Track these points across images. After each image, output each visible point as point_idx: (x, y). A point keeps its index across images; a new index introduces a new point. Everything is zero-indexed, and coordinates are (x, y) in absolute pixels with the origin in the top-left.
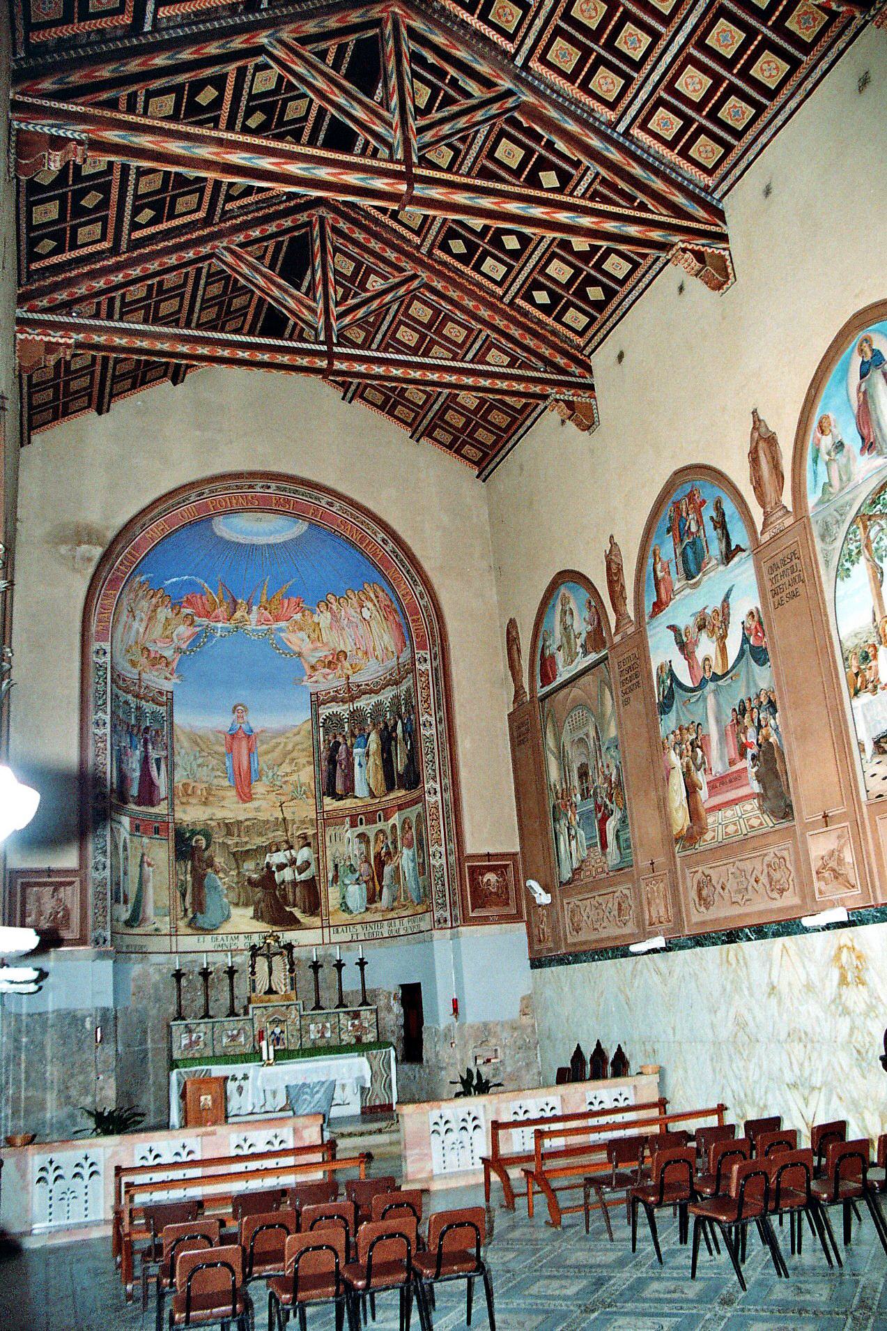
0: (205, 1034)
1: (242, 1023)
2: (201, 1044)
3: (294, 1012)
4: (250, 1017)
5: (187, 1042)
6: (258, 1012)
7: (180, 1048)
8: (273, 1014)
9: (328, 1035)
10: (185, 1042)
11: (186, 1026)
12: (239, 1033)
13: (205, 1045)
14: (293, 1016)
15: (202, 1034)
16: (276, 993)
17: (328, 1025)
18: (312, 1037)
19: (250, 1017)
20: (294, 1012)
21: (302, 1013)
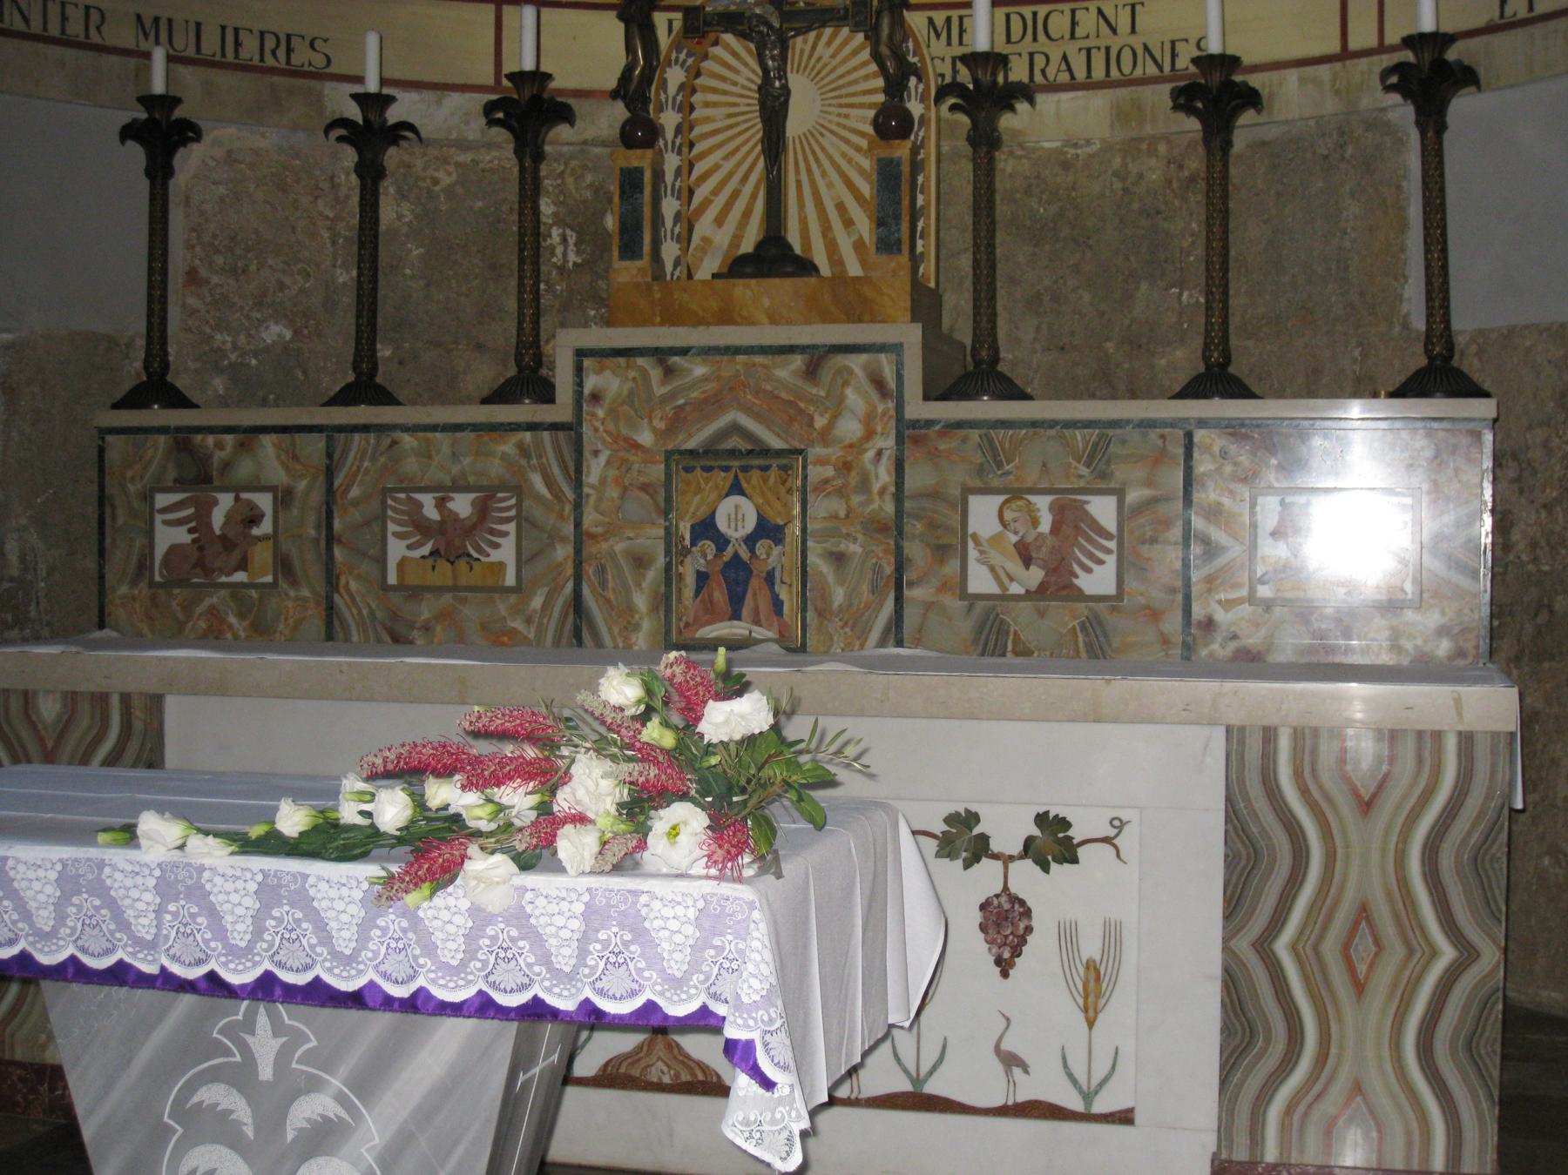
0: (284, 498)
1: (508, 446)
2: (262, 555)
3: (856, 399)
4: (561, 411)
5: (182, 536)
6: (605, 381)
7: (144, 565)
8: (711, 404)
9: (1098, 580)
10: (169, 536)
11: (183, 440)
12: (483, 510)
13: (284, 565)
14: (849, 428)
15: (264, 501)
16: (805, 267)
17: (1103, 509)
18: (980, 581)
19: (561, 411)
20: (856, 399)
21: (917, 408)
